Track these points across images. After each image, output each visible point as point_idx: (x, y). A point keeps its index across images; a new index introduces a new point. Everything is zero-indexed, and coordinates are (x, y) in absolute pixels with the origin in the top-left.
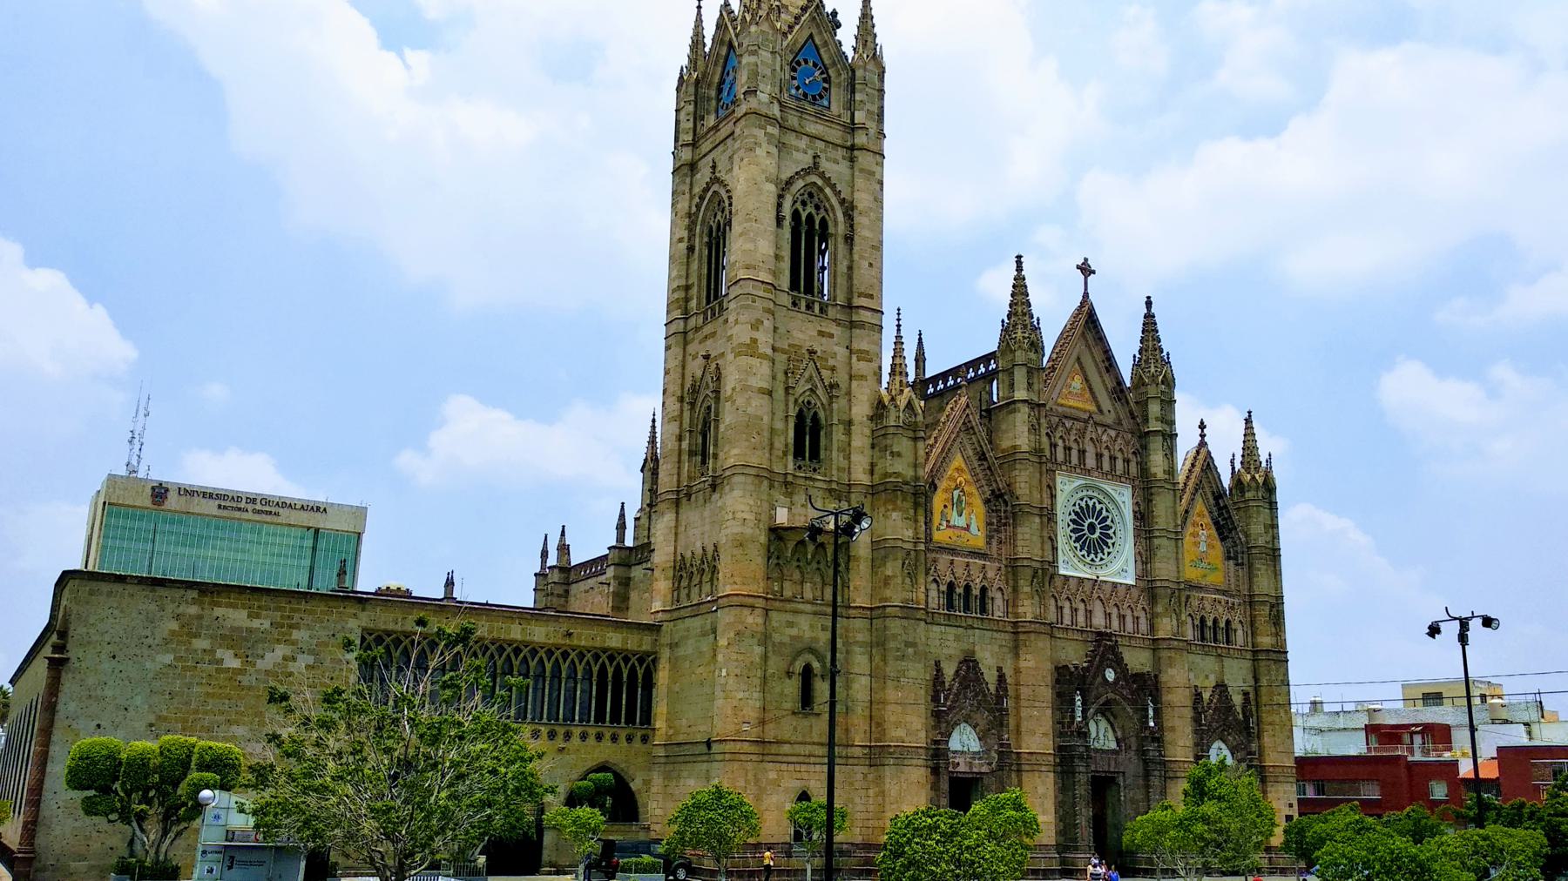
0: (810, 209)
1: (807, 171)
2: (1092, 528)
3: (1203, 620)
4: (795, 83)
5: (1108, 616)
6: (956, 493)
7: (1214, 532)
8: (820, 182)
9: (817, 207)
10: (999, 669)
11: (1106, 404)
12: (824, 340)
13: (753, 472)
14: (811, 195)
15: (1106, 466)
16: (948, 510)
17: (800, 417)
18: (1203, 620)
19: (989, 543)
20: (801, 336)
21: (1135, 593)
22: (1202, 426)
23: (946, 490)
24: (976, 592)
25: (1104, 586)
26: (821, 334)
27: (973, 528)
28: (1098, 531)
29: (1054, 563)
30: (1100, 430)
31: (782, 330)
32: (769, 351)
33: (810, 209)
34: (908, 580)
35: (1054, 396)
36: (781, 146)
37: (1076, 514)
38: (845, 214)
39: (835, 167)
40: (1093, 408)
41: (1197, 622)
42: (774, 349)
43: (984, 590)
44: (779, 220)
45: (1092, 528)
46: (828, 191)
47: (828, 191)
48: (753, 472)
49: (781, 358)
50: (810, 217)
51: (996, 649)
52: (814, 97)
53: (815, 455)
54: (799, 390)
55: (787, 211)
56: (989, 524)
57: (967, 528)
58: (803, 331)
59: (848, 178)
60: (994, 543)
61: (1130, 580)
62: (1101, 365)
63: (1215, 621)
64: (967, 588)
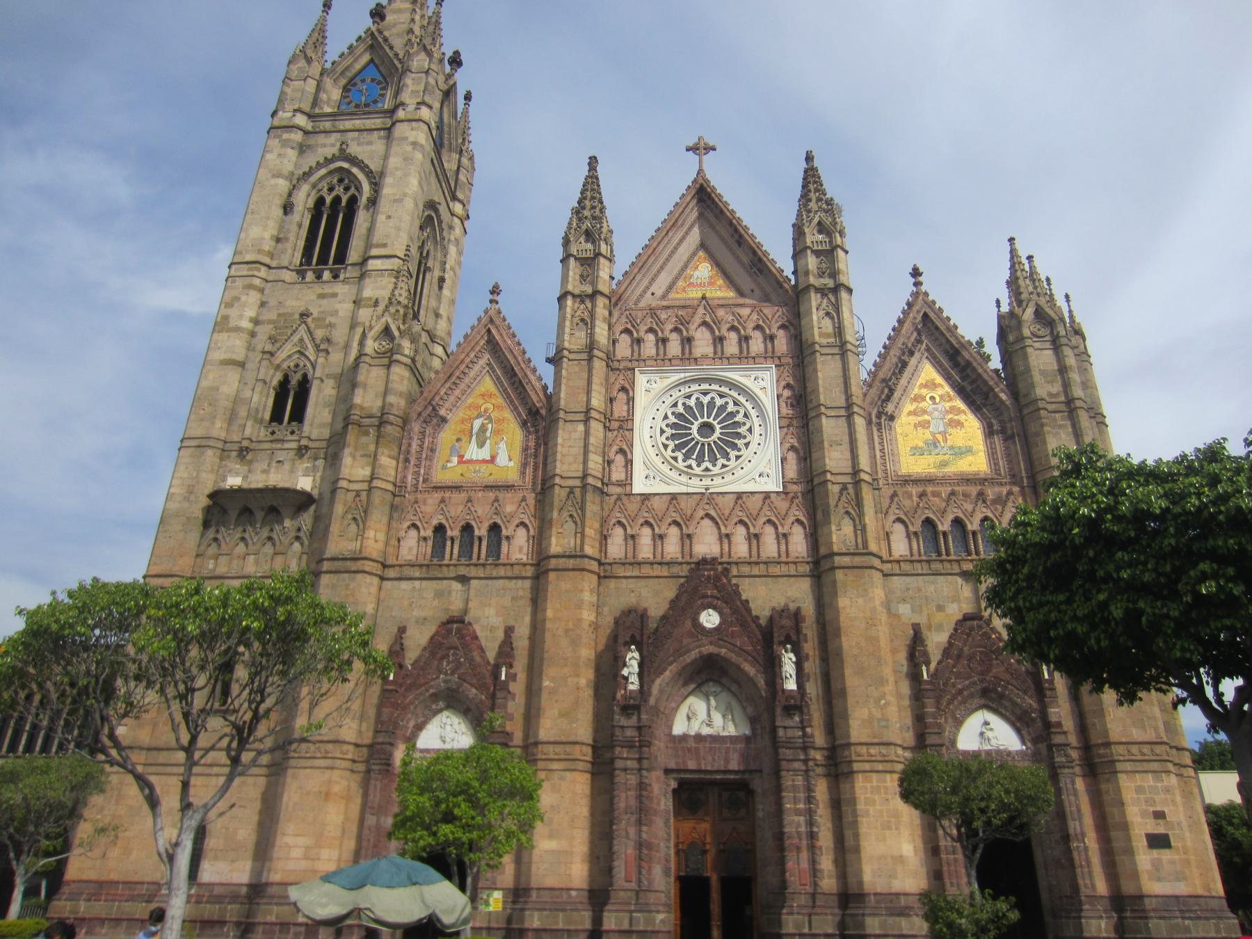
0: (339, 190)
1: (334, 159)
2: (707, 428)
3: (928, 522)
4: (347, 100)
5: (726, 538)
6: (477, 424)
7: (959, 404)
8: (346, 165)
9: (347, 189)
10: (509, 631)
11: (746, 282)
12: (324, 302)
13: (195, 443)
14: (341, 181)
15: (731, 347)
16: (463, 443)
17: (285, 383)
18: (928, 522)
19: (523, 473)
20: (294, 303)
21: (782, 505)
22: (916, 273)
23: (463, 421)
24: (481, 531)
25: (719, 499)
26: (322, 296)
27: (502, 460)
28: (717, 434)
29: (627, 482)
30: (721, 313)
31: (273, 302)
32: (246, 324)
33: (339, 190)
34: (353, 527)
35: (659, 287)
36: (302, 149)
37: (679, 416)
38: (371, 183)
39: (368, 149)
40: (732, 294)
41: (916, 526)
42: (256, 321)
43: (495, 528)
44: (287, 208)
45: (707, 428)
46: (355, 170)
47: (355, 170)
48: (195, 443)
49: (264, 331)
50: (337, 200)
51: (507, 601)
52: (367, 105)
53: (298, 415)
54: (282, 355)
55: (304, 199)
56: (525, 449)
57: (493, 459)
58: (303, 297)
59: (382, 152)
60: (529, 471)
61: (773, 485)
62: (732, 242)
63: (958, 522)
64: (467, 528)
